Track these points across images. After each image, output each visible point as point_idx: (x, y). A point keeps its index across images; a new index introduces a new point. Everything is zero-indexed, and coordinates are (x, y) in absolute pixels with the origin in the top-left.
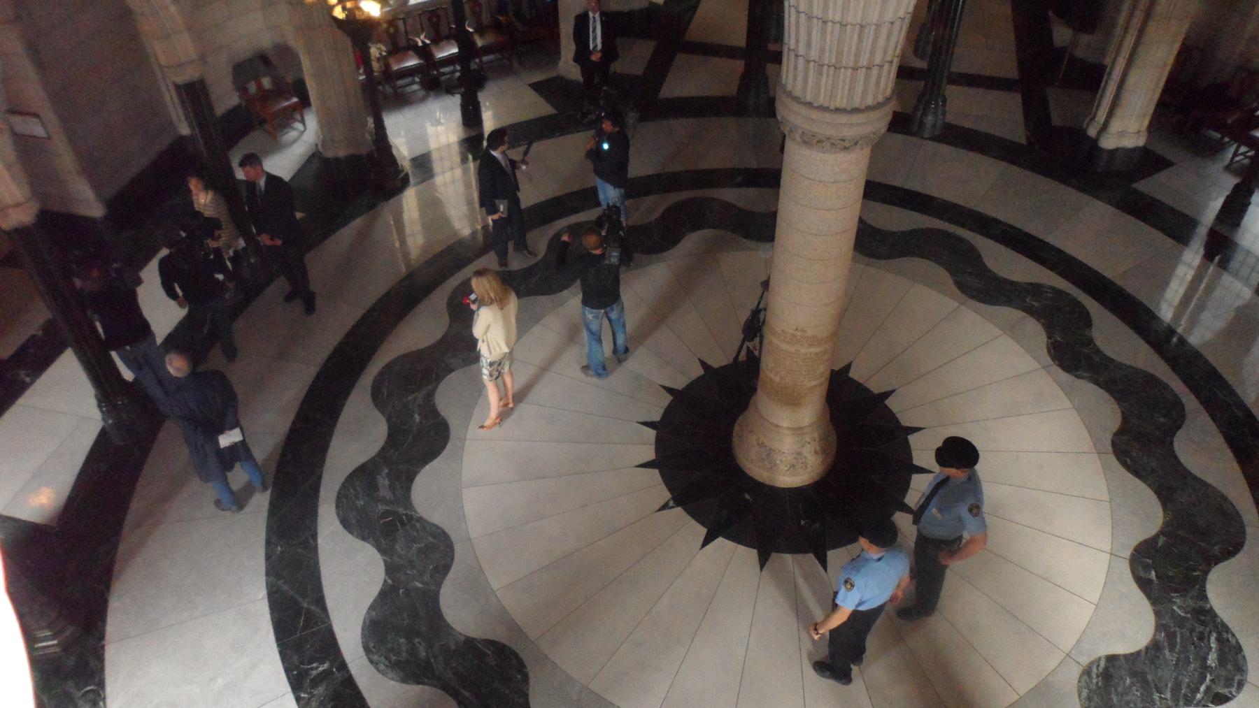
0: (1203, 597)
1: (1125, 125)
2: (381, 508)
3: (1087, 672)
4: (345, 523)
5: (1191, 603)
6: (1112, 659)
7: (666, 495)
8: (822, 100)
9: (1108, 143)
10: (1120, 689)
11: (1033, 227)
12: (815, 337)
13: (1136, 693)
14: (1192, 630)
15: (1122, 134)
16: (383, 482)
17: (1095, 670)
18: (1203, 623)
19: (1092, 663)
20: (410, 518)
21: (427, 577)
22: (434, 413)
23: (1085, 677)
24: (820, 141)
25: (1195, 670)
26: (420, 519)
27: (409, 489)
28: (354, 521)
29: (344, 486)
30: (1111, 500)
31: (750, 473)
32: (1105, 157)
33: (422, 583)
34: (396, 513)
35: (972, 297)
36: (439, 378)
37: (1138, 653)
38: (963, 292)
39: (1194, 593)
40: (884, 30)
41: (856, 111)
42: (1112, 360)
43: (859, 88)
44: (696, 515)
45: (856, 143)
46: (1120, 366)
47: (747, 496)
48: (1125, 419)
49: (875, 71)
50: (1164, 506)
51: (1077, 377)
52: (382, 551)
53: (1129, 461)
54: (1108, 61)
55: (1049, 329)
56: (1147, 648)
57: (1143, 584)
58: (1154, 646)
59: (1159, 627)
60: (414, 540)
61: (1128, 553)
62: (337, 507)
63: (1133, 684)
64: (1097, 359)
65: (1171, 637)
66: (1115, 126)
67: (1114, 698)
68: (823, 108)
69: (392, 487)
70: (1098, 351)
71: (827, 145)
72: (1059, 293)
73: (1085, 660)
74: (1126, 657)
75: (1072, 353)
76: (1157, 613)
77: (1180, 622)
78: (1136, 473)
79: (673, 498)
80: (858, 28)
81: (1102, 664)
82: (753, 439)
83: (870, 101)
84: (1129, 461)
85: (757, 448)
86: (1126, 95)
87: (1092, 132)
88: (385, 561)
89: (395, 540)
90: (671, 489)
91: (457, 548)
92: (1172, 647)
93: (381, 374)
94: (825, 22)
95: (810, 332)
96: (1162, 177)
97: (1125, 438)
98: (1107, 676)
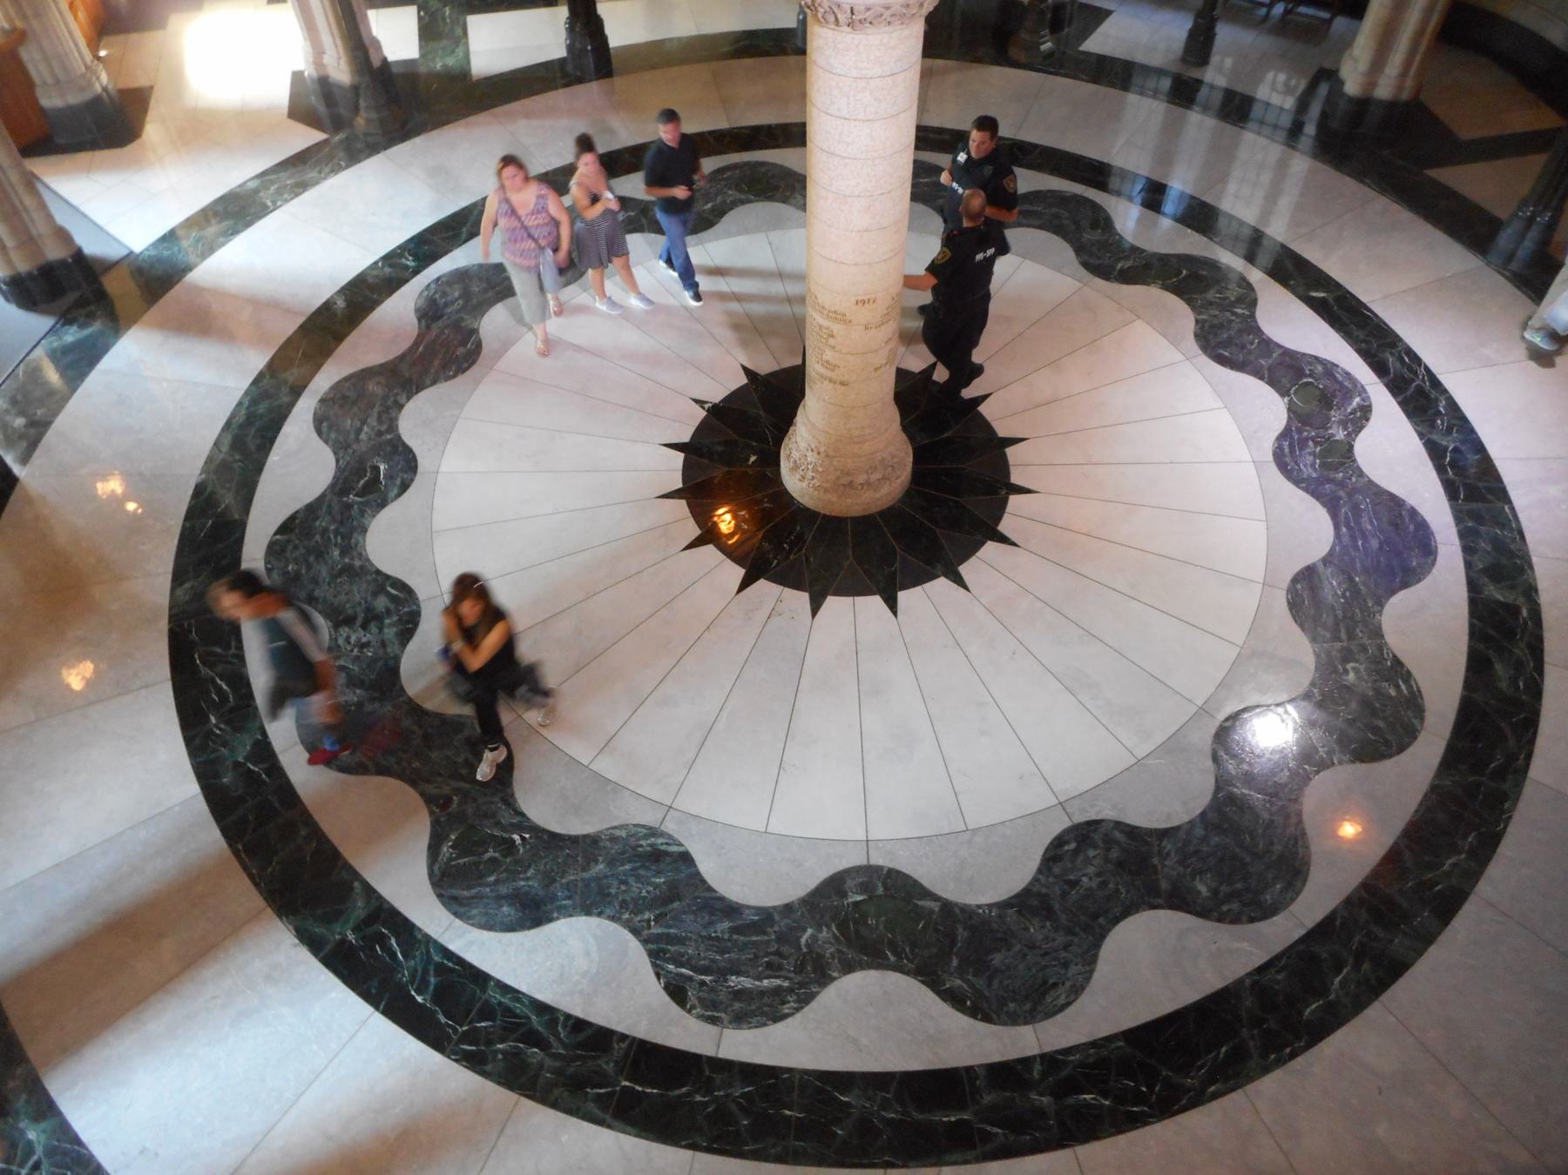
0: (848, 968)
3: (653, 832)
6: (686, 858)
10: (642, 872)
14: (778, 953)
17: (660, 841)
18: (800, 969)
19: (670, 837)
25: (713, 961)
37: (710, 889)
50: (1004, 905)
56: (722, 899)
63: (656, 886)
67: (627, 867)
73: (670, 827)
74: (698, 874)
76: (788, 908)
92: (734, 930)
93: (747, 164)
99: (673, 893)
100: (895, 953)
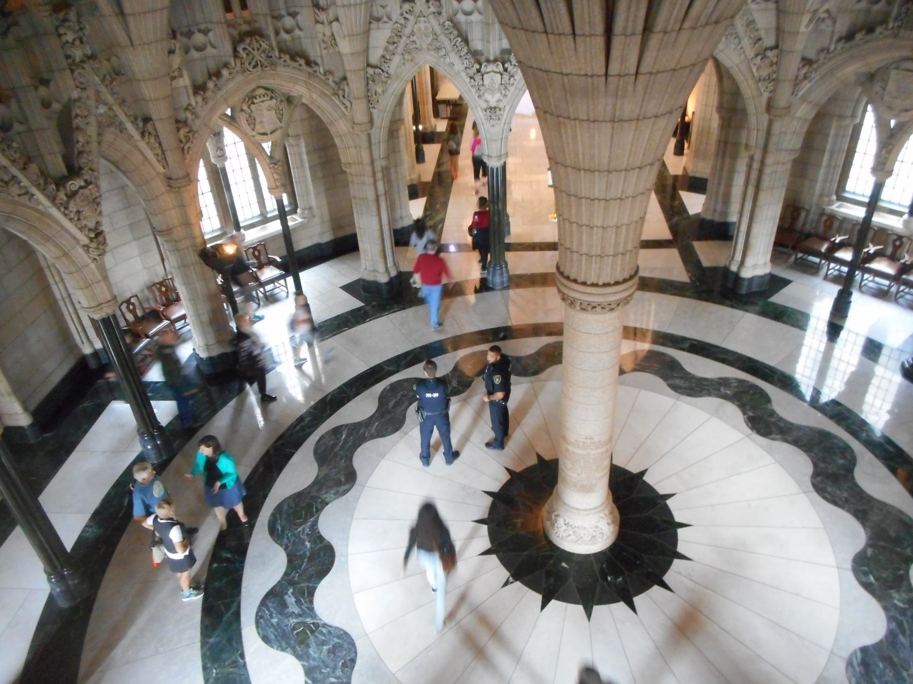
1: (756, 261)
2: (293, 621)
3: (850, 664)
4: (266, 639)
5: (904, 595)
6: (864, 650)
7: (504, 574)
8: (592, 279)
9: (746, 274)
10: (878, 673)
11: (712, 338)
12: (600, 442)
13: (889, 675)
15: (755, 266)
16: (290, 600)
20: (317, 625)
21: (339, 672)
22: (321, 538)
23: (850, 668)
24: (594, 307)
26: (325, 625)
27: (311, 602)
28: (272, 637)
29: (259, 609)
30: (825, 527)
31: (562, 547)
32: (746, 283)
33: (336, 678)
34: (304, 623)
35: (682, 393)
36: (319, 511)
37: (881, 641)
38: (676, 391)
39: (904, 588)
40: (632, 226)
41: (617, 283)
42: (792, 424)
43: (619, 269)
44: (533, 585)
45: (618, 305)
46: (799, 428)
47: (564, 565)
48: (815, 465)
49: (628, 255)
50: (864, 526)
51: (773, 439)
52: (299, 657)
53: (828, 496)
54: (733, 218)
55: (742, 407)
56: (886, 637)
57: (867, 587)
58: (891, 636)
59: (890, 619)
60: (323, 643)
61: (849, 565)
62: (257, 627)
63: (885, 668)
64: (782, 425)
65: (900, 625)
66: (749, 262)
68: (594, 285)
69: (298, 602)
70: (781, 419)
71: (598, 309)
72: (741, 382)
73: (846, 654)
75: (763, 422)
77: (903, 612)
78: (835, 502)
79: (512, 575)
80: (614, 229)
81: (859, 655)
82: (561, 522)
83: (627, 275)
84: (828, 496)
85: (564, 527)
86: (752, 241)
87: (734, 268)
88: (303, 666)
89: (308, 646)
90: (509, 571)
91: (357, 643)
92: (903, 633)
93: (273, 515)
94: (592, 228)
95: (596, 439)
96: (786, 291)
97: (819, 479)
98: (865, 663)
99: (888, 660)
100: (899, 569)
